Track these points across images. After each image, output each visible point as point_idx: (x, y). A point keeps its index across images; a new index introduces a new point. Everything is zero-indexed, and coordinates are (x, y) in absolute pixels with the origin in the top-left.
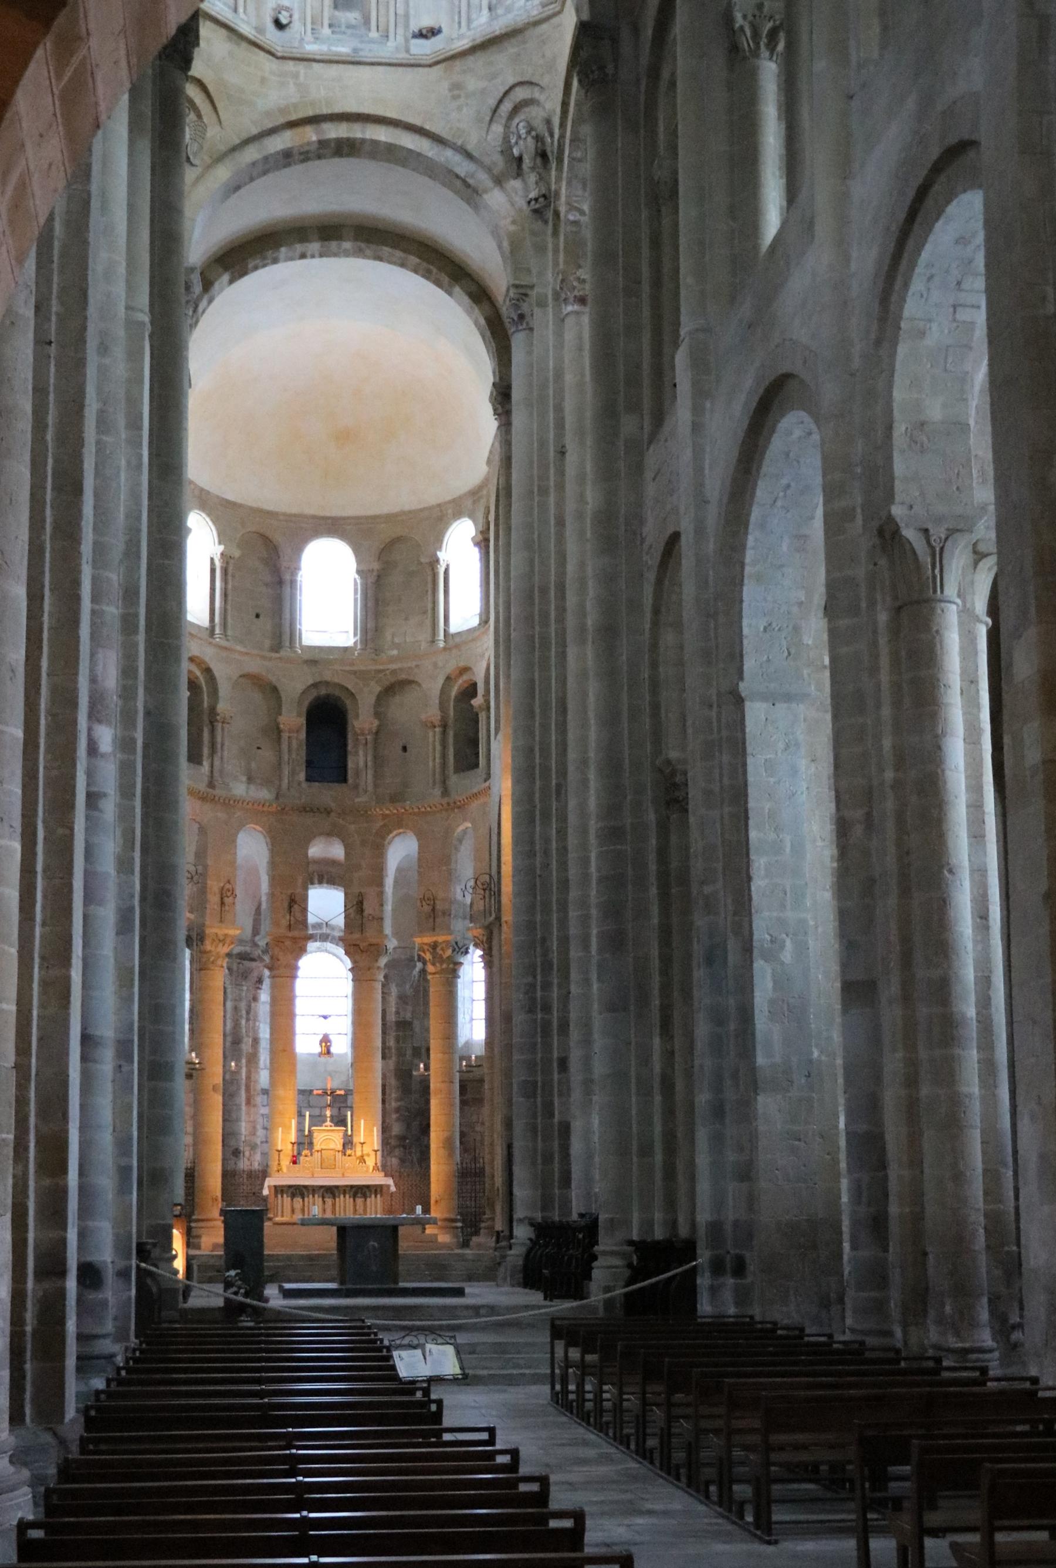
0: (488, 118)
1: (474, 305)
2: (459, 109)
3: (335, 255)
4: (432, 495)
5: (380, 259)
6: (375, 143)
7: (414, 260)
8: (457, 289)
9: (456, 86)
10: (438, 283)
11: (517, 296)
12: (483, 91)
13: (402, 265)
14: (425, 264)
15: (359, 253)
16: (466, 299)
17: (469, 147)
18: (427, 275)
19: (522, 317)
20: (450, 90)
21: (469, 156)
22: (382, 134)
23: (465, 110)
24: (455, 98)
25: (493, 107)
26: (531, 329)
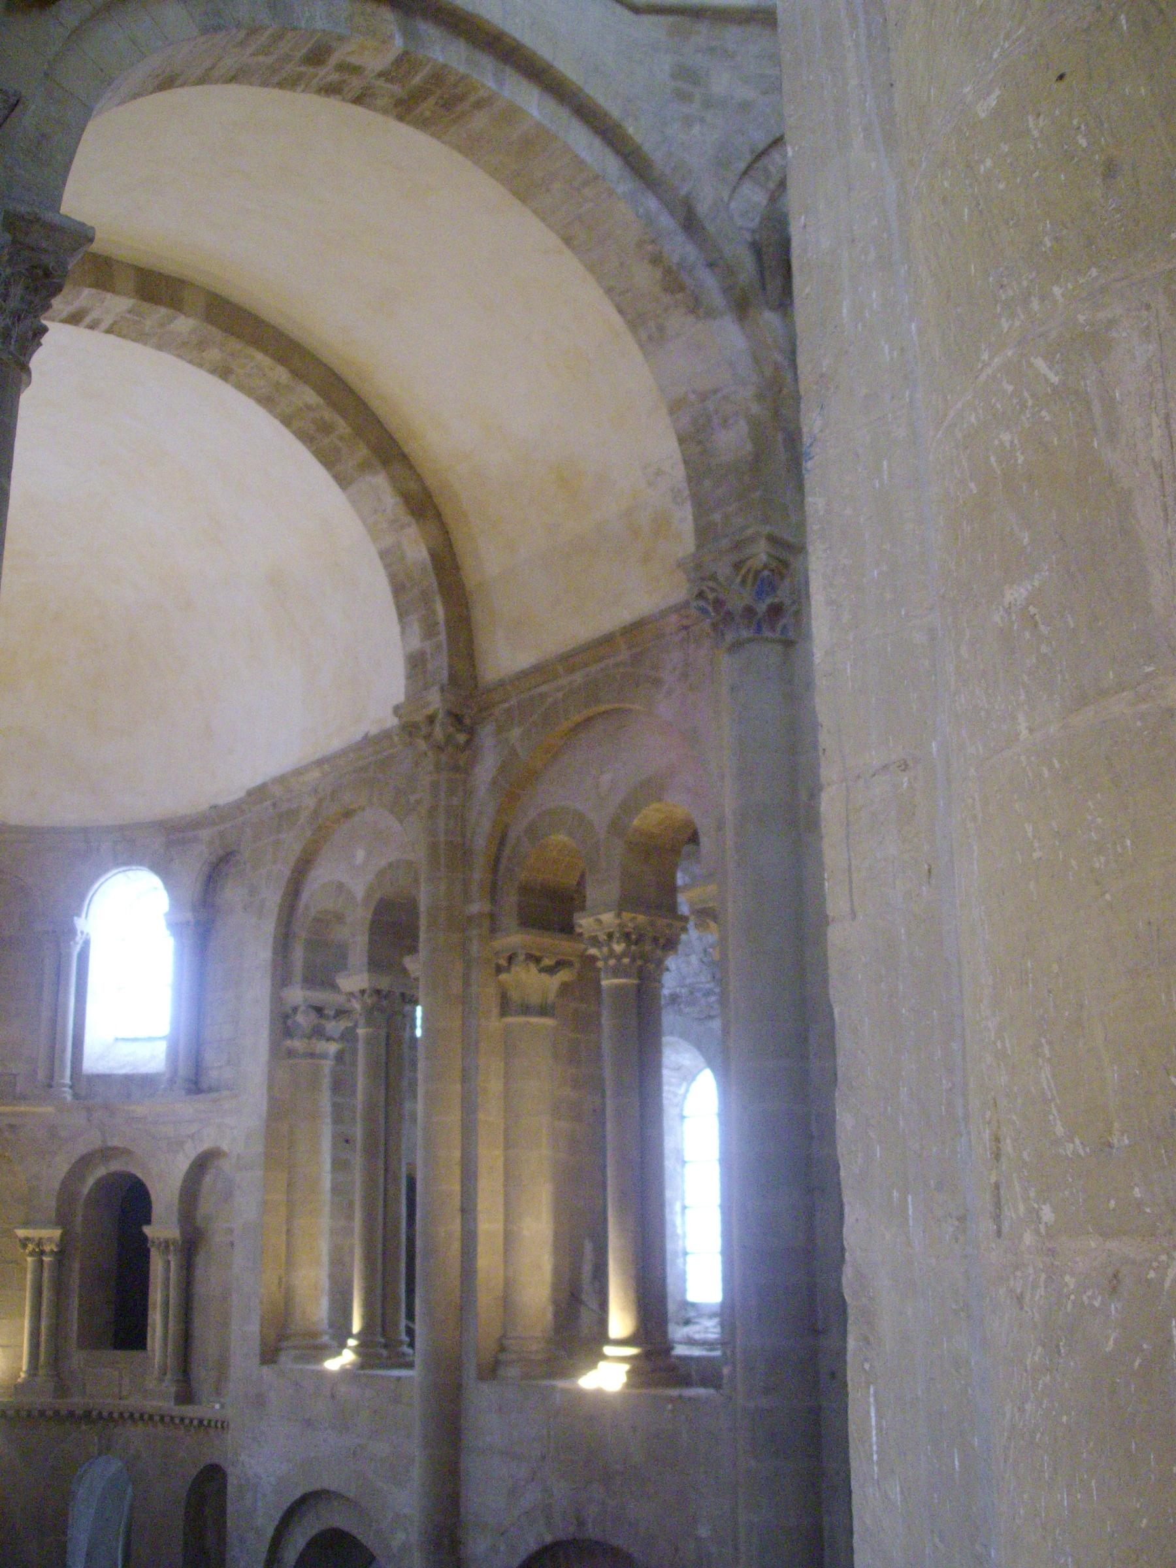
0: (742, 166)
1: (408, 519)
2: (688, 121)
3: (141, 337)
4: (66, 808)
5: (224, 373)
6: (511, 114)
7: (310, 397)
8: (380, 481)
9: (686, 74)
10: (328, 459)
11: (774, 564)
12: (745, 107)
13: (266, 402)
14: (328, 415)
15: (191, 350)
16: (390, 501)
17: (702, 208)
18: (313, 436)
19: (776, 611)
20: (674, 77)
21: (691, 224)
22: (533, 103)
23: (696, 129)
24: (683, 97)
25: (761, 147)
26: (789, 644)
